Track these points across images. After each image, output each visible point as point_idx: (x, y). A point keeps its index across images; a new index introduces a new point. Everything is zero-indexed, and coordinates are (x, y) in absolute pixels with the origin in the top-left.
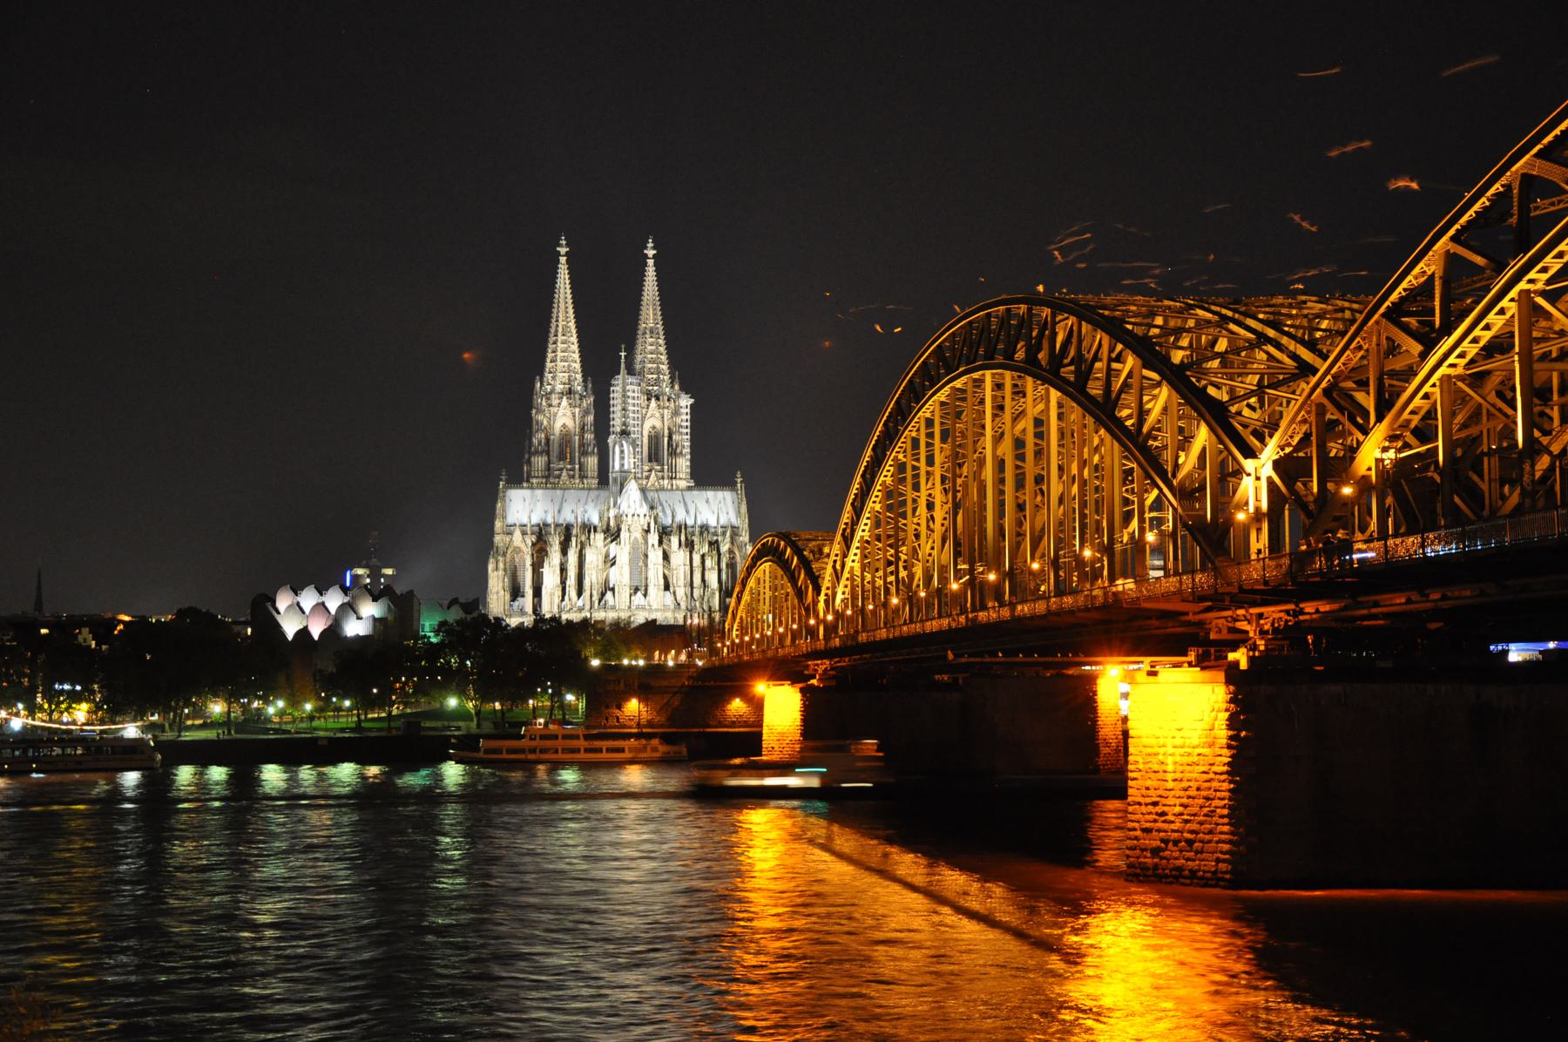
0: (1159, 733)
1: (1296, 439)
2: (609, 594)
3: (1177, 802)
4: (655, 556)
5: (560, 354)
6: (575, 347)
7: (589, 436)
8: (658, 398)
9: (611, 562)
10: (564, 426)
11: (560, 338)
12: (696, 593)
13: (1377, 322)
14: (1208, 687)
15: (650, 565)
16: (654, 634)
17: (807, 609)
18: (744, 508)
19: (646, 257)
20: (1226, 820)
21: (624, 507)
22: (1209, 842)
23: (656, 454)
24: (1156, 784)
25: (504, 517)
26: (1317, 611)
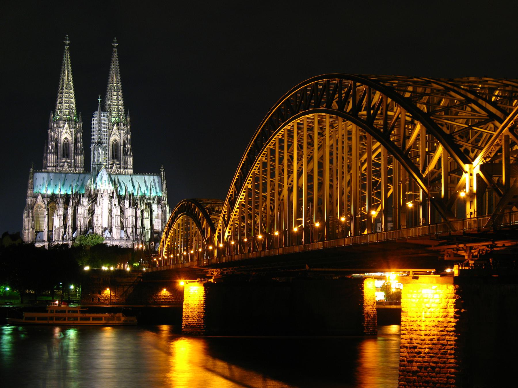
1: (493, 154)
2: (91, 231)
3: (427, 346)
4: (116, 211)
5: (64, 99)
6: (72, 95)
7: (79, 145)
8: (118, 125)
9: (91, 212)
10: (66, 138)
11: (65, 90)
12: (138, 231)
14: (445, 286)
15: (113, 216)
16: (116, 254)
17: (207, 241)
18: (164, 186)
19: (113, 47)
20: (453, 356)
22: (444, 368)
23: (117, 155)
25: (33, 188)
26: (504, 246)
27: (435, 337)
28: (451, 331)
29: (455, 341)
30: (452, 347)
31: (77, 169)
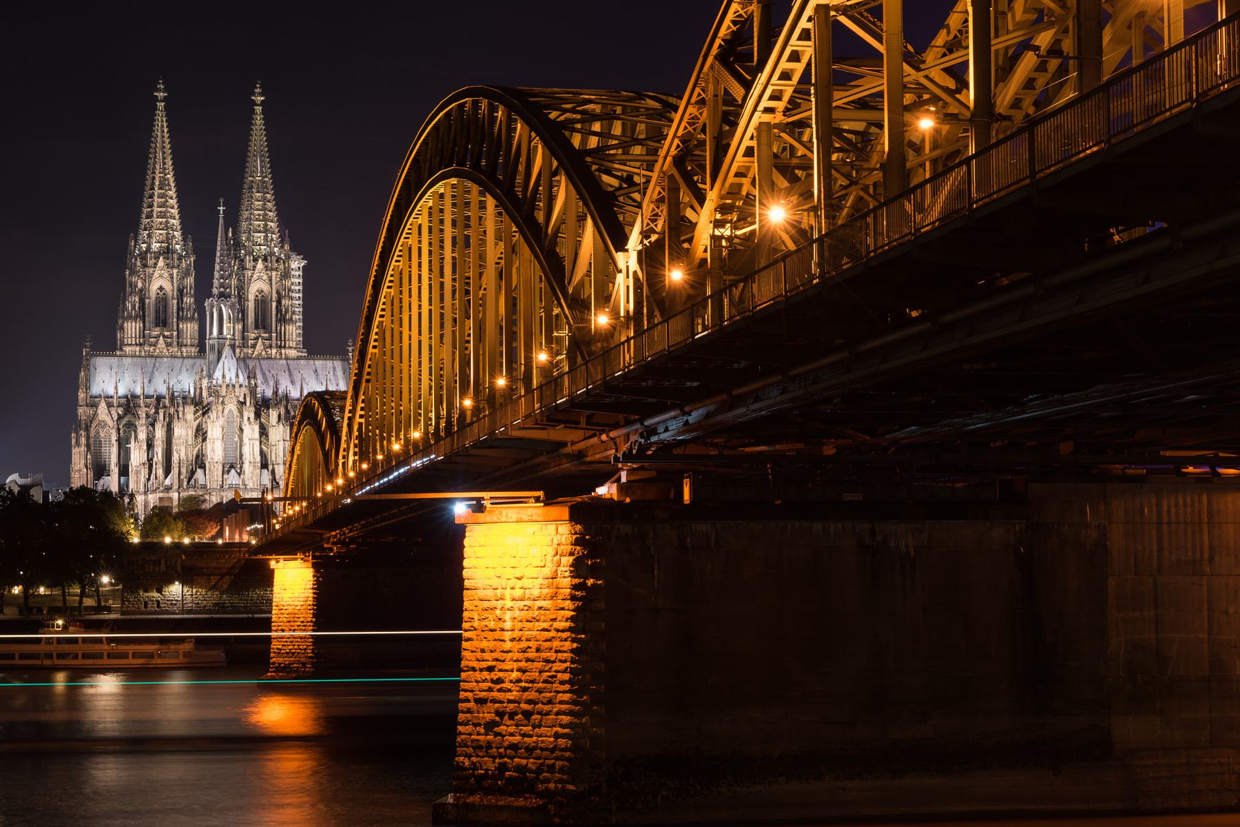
0: (495, 582)
3: (515, 665)
13: (712, 67)
14: (552, 527)
20: (567, 687)
21: (218, 374)
22: (548, 713)
24: (491, 645)
27: (530, 644)
28: (563, 631)
29: (572, 651)
30: (568, 664)
31: (184, 350)
